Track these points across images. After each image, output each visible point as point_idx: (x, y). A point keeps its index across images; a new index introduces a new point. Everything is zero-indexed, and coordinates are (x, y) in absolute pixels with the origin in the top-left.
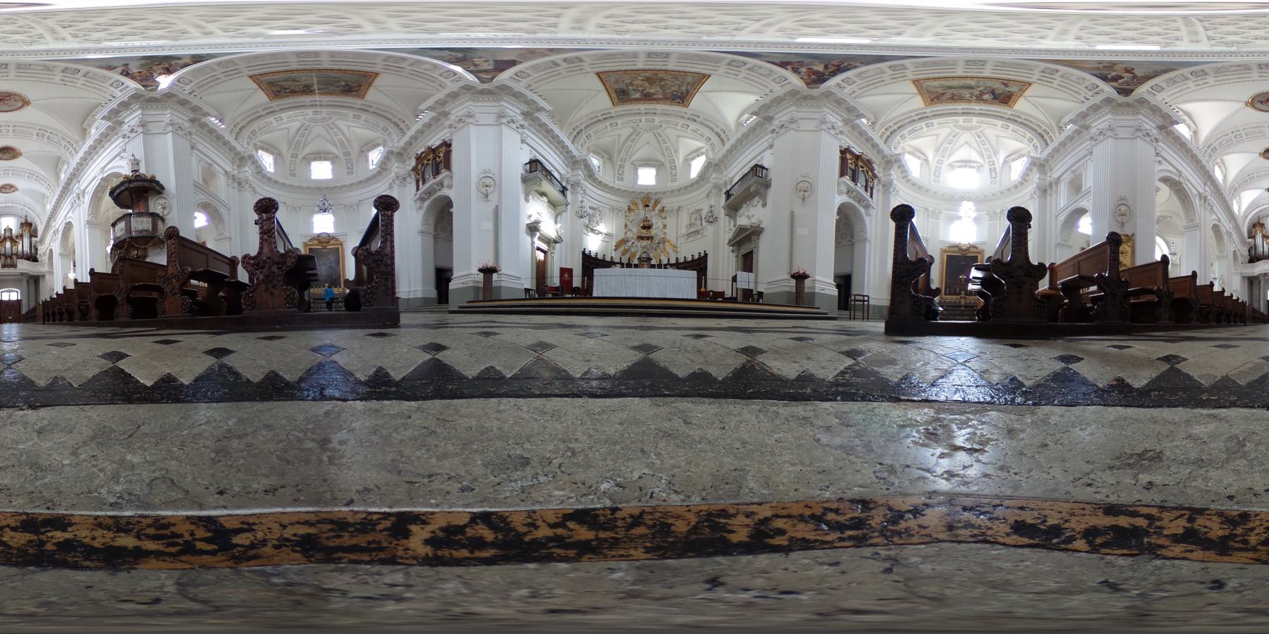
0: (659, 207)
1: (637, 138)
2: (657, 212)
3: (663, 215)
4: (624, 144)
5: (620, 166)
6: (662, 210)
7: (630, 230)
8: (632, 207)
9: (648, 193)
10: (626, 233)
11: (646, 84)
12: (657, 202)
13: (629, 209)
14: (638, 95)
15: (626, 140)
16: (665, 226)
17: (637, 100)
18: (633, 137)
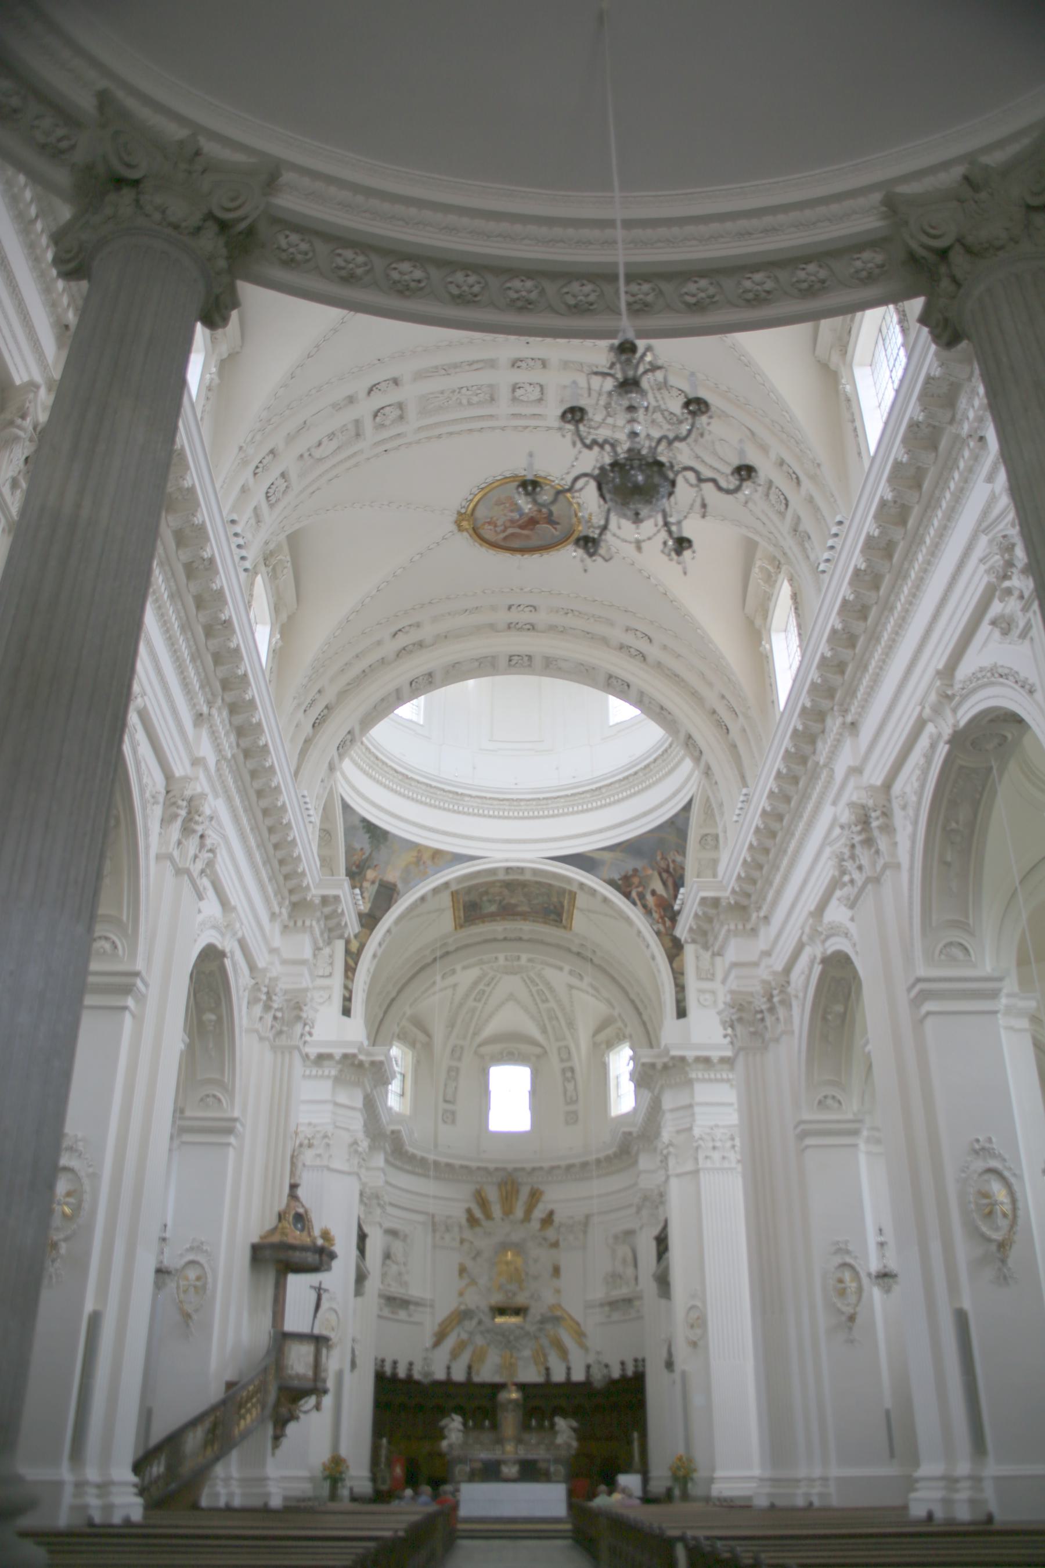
0: (539, 1213)
1: (488, 989)
2: (535, 1225)
3: (551, 1233)
4: (461, 1005)
5: (450, 1069)
6: (548, 1220)
7: (473, 1282)
8: (478, 1213)
9: (516, 1170)
10: (461, 1294)
11: (506, 892)
12: (535, 1196)
13: (472, 1221)
14: (493, 908)
15: (467, 996)
16: (556, 1271)
17: (492, 917)
18: (481, 987)
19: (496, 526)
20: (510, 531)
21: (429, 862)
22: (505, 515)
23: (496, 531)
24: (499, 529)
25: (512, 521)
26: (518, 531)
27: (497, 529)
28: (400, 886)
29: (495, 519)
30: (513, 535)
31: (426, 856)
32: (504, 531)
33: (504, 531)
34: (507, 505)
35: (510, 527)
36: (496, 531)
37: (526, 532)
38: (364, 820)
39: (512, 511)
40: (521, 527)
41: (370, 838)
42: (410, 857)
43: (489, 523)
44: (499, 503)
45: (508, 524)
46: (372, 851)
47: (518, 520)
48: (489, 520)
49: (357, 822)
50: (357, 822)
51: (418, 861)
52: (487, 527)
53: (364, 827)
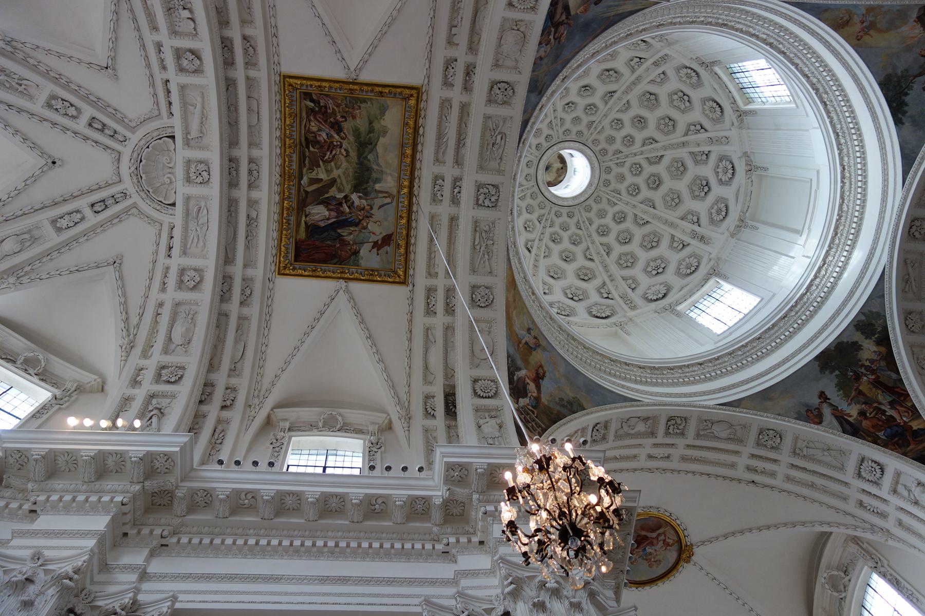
19: (664, 540)
20: (654, 535)
21: (856, 19)
22: (655, 550)
23: (665, 536)
24: (662, 537)
25: (652, 544)
26: (649, 535)
27: (664, 538)
28: (915, 15)
29: (664, 548)
30: (653, 531)
31: (856, 28)
32: (659, 535)
33: (659, 535)
34: (653, 560)
35: (654, 538)
36: (665, 536)
37: (644, 533)
38: (898, 122)
39: (650, 554)
40: (646, 538)
41: (906, 94)
42: (875, 39)
43: (668, 545)
44: (658, 562)
45: (655, 542)
46: (916, 77)
47: (648, 544)
48: (668, 548)
49: (907, 125)
50: (907, 125)
51: (870, 27)
52: (671, 541)
53: (904, 113)
